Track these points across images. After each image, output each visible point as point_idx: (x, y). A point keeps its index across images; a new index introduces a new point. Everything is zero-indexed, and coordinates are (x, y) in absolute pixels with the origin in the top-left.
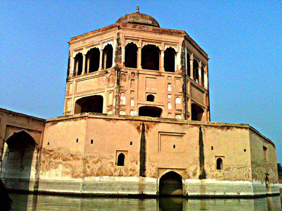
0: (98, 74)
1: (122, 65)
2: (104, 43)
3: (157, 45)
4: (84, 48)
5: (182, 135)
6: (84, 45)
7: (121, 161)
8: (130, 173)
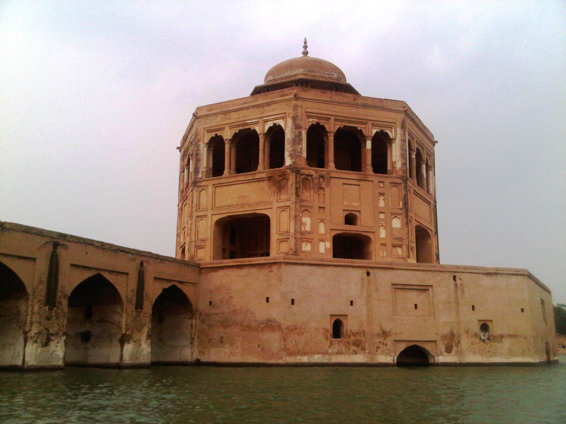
0: (258, 176)
1: (303, 163)
2: (267, 121)
3: (359, 127)
4: (227, 127)
5: (424, 289)
6: (227, 122)
8: (354, 348)
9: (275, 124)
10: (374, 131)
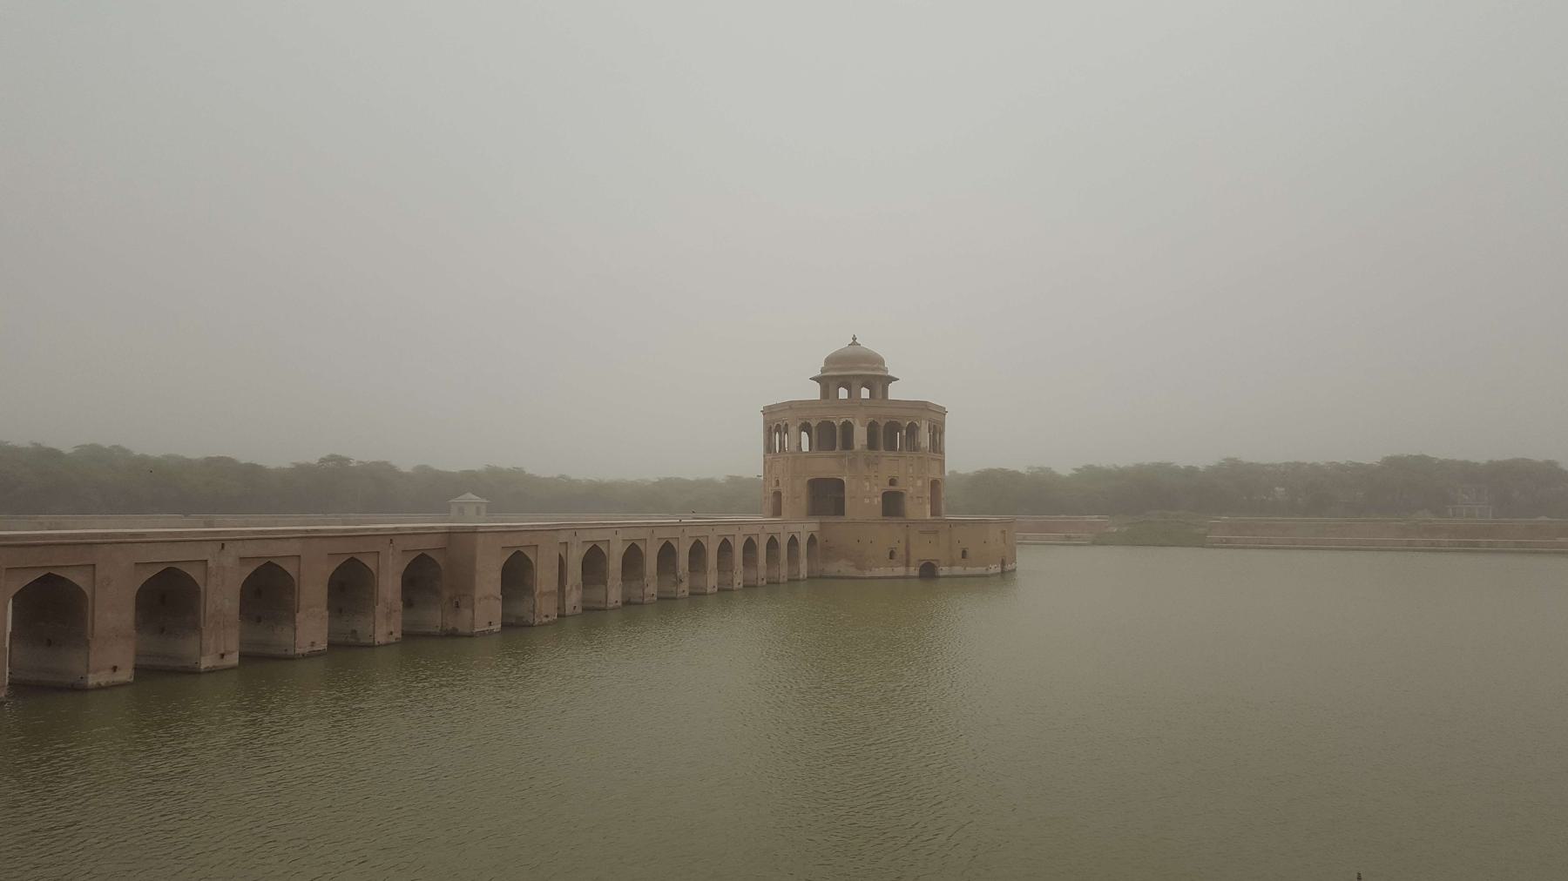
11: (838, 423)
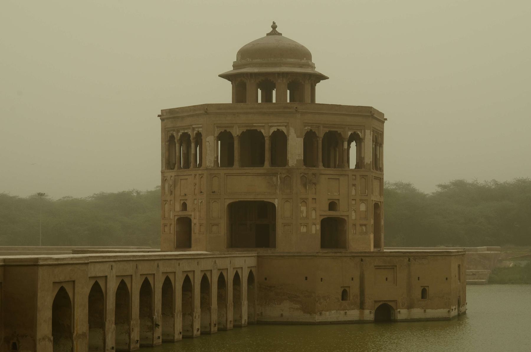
7: (345, 295)
9: (278, 130)
10: (350, 133)
11: (267, 132)
